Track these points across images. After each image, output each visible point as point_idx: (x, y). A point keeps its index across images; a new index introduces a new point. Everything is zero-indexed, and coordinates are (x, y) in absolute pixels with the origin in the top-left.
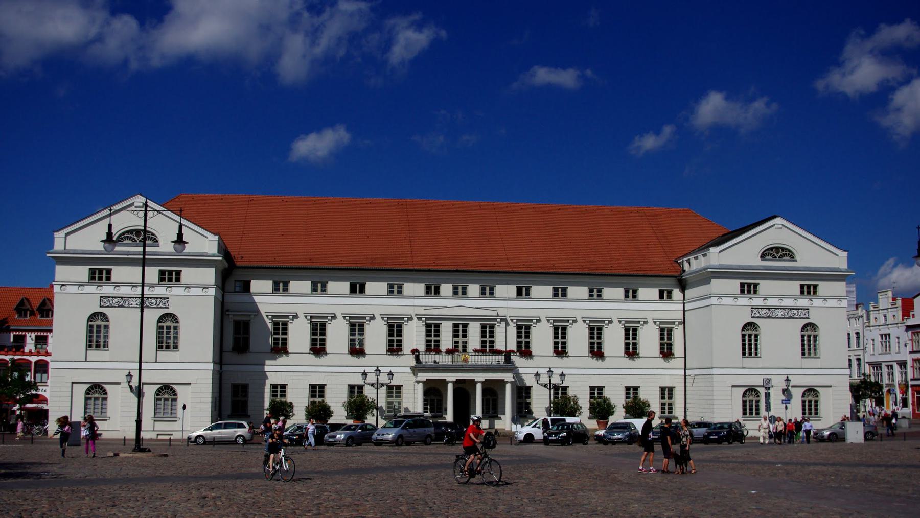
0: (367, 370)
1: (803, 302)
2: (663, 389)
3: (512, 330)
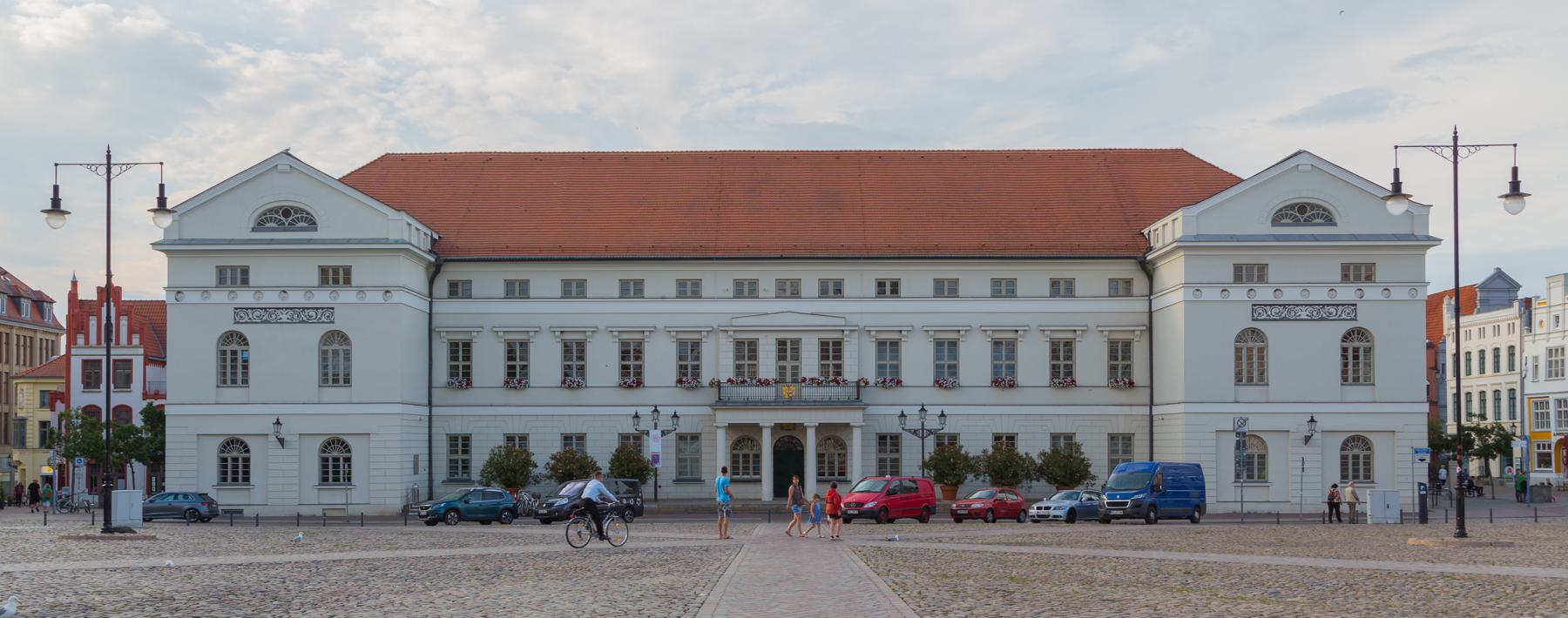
0: (641, 411)
1: (1346, 293)
2: (1113, 438)
3: (871, 349)
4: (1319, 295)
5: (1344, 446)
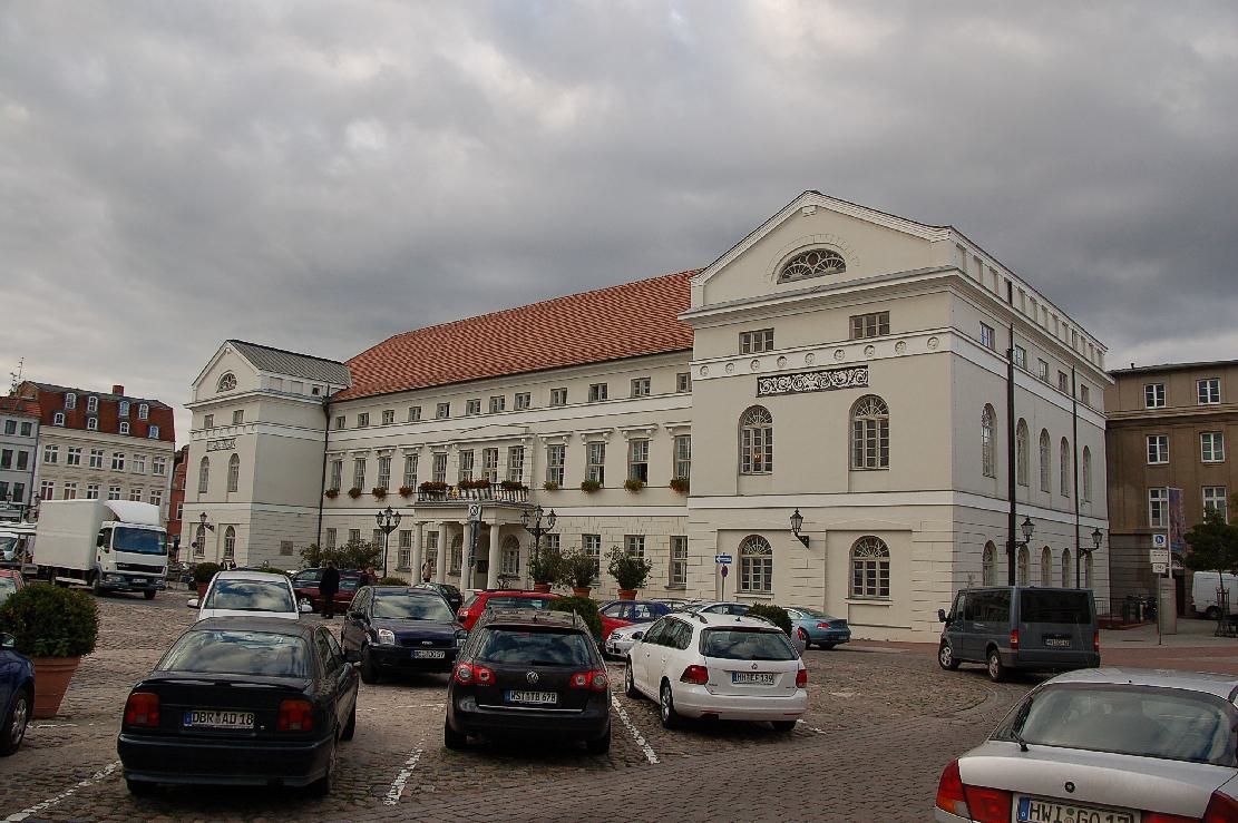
4: (825, 359)
5: (856, 550)
